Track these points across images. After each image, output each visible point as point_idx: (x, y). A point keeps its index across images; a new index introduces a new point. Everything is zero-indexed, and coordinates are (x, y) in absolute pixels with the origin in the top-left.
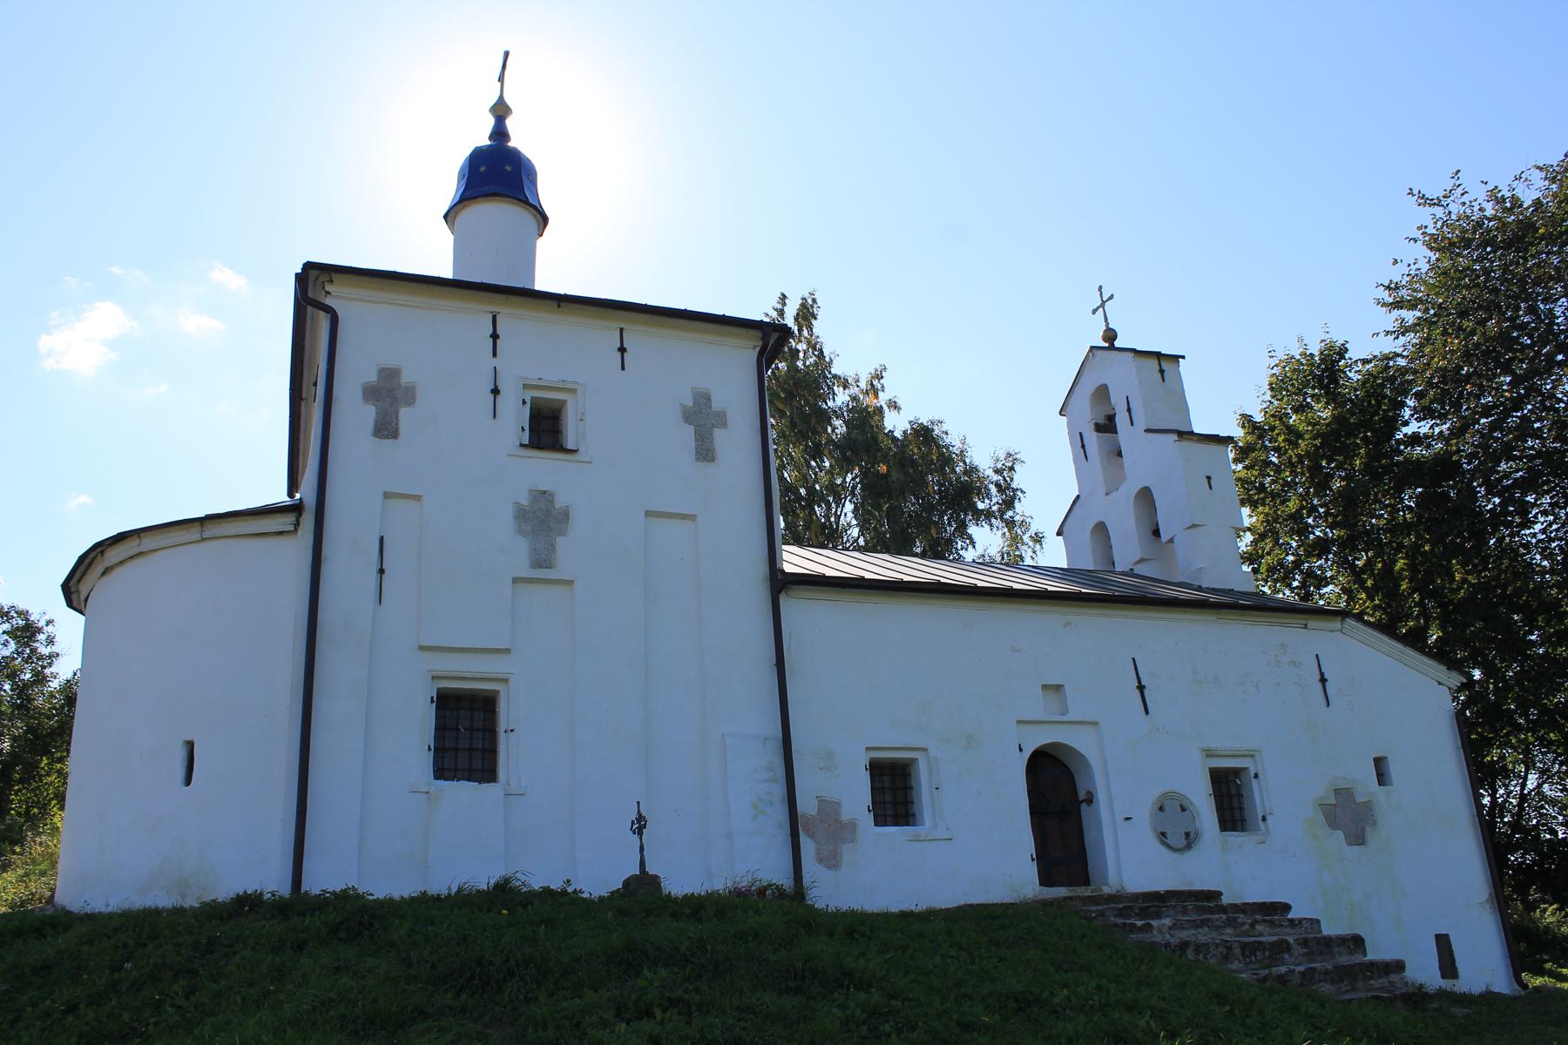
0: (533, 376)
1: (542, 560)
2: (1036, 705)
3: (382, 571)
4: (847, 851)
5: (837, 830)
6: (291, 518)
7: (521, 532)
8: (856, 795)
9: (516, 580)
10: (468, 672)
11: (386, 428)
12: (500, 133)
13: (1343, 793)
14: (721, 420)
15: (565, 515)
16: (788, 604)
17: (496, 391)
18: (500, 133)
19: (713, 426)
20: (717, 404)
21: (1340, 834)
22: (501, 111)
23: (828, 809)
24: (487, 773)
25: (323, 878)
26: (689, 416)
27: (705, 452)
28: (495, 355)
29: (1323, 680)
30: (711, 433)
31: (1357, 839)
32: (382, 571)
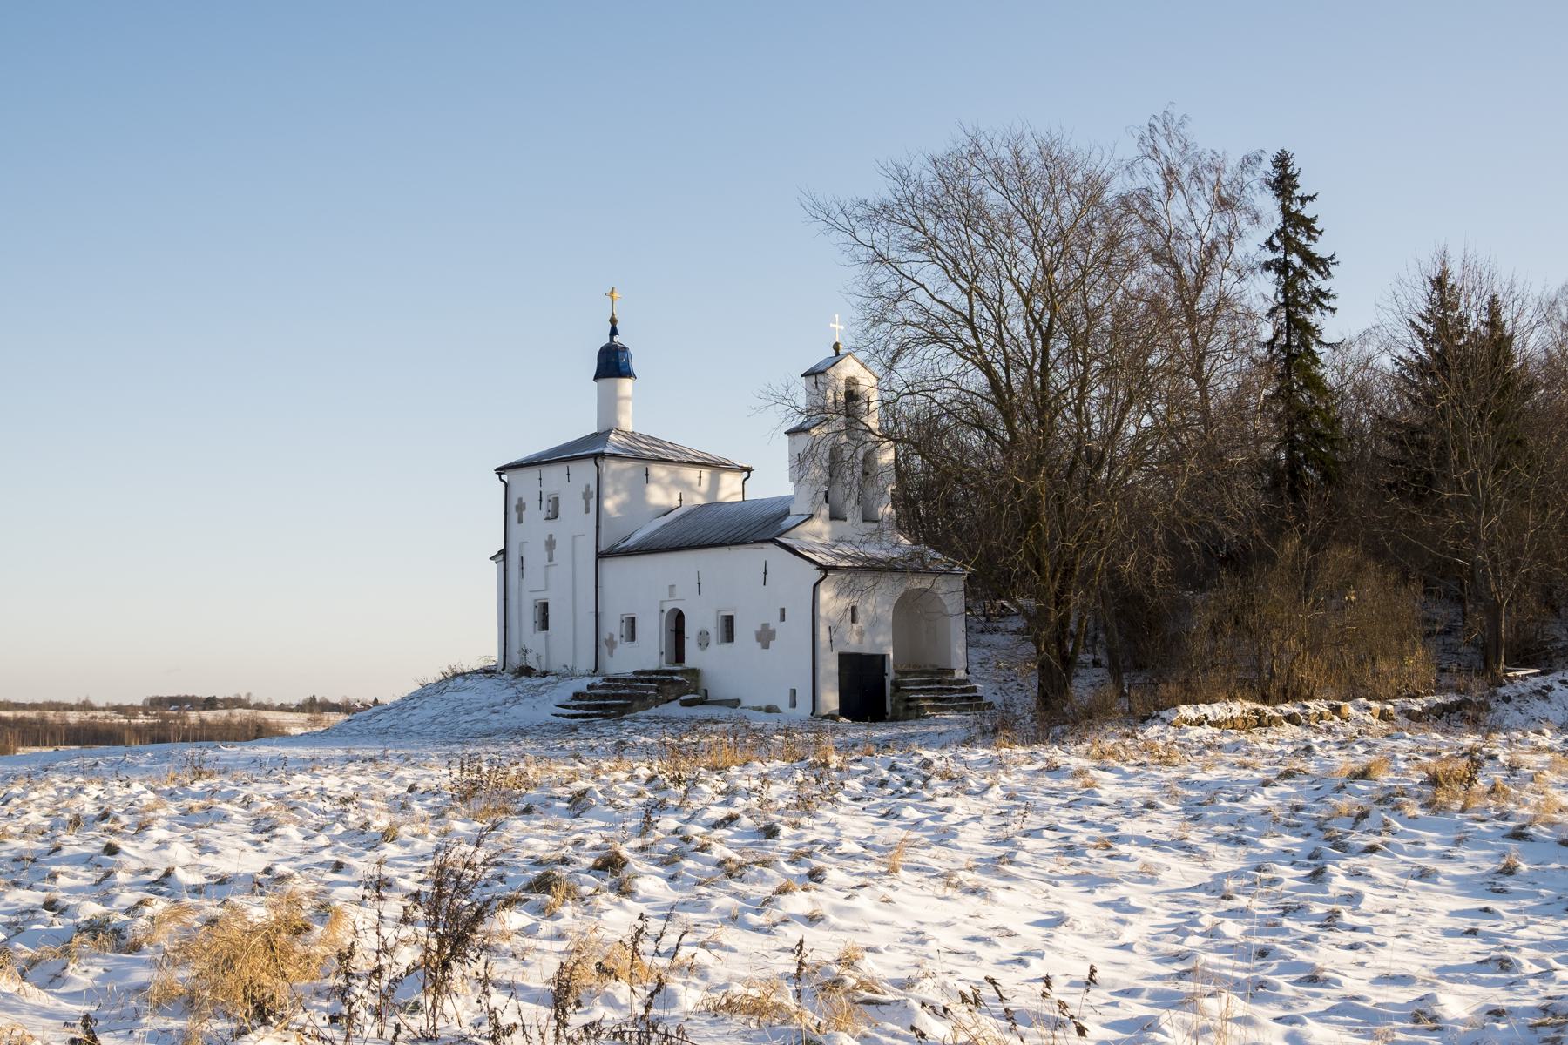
1: (550, 560)
11: (520, 521)
13: (765, 626)
29: (765, 573)
31: (766, 646)
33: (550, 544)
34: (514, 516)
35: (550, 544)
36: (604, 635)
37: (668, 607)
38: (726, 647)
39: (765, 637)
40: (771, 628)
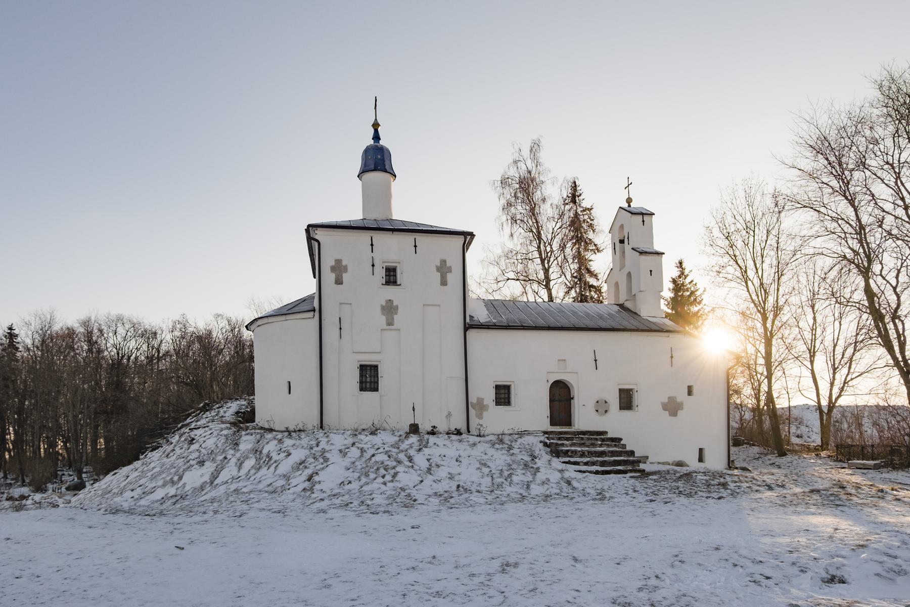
1: (390, 323)
3: (341, 329)
4: (485, 414)
6: (312, 313)
7: (383, 314)
9: (382, 330)
10: (369, 359)
11: (339, 281)
12: (376, 137)
14: (450, 270)
15: (397, 307)
16: (471, 334)
17: (373, 265)
18: (376, 137)
19: (447, 272)
20: (448, 264)
21: (667, 412)
22: (376, 126)
27: (444, 283)
28: (372, 252)
30: (446, 275)
32: (341, 329)
33: (390, 309)
34: (329, 277)
35: (390, 309)
36: (473, 399)
38: (626, 413)
39: (672, 408)
40: (679, 400)
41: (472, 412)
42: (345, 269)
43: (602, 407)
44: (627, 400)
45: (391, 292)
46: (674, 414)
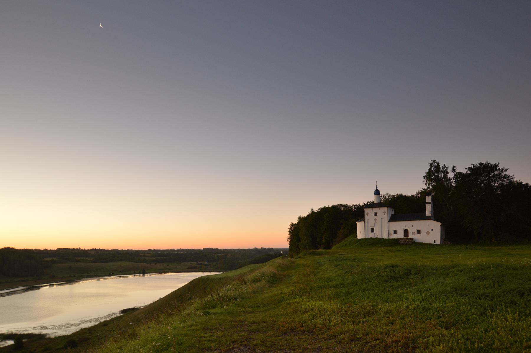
0: (375, 211)
2: (404, 227)
4: (392, 236)
5: (391, 234)
8: (392, 232)
10: (372, 227)
11: (367, 216)
23: (391, 233)
24: (374, 232)
25: (367, 237)
26: (383, 212)
27: (384, 214)
33: (375, 220)
35: (375, 220)
36: (390, 233)
37: (404, 229)
39: (428, 233)
41: (390, 235)
42: (368, 214)
43: (413, 233)
44: (419, 232)
45: (376, 217)
46: (428, 234)
